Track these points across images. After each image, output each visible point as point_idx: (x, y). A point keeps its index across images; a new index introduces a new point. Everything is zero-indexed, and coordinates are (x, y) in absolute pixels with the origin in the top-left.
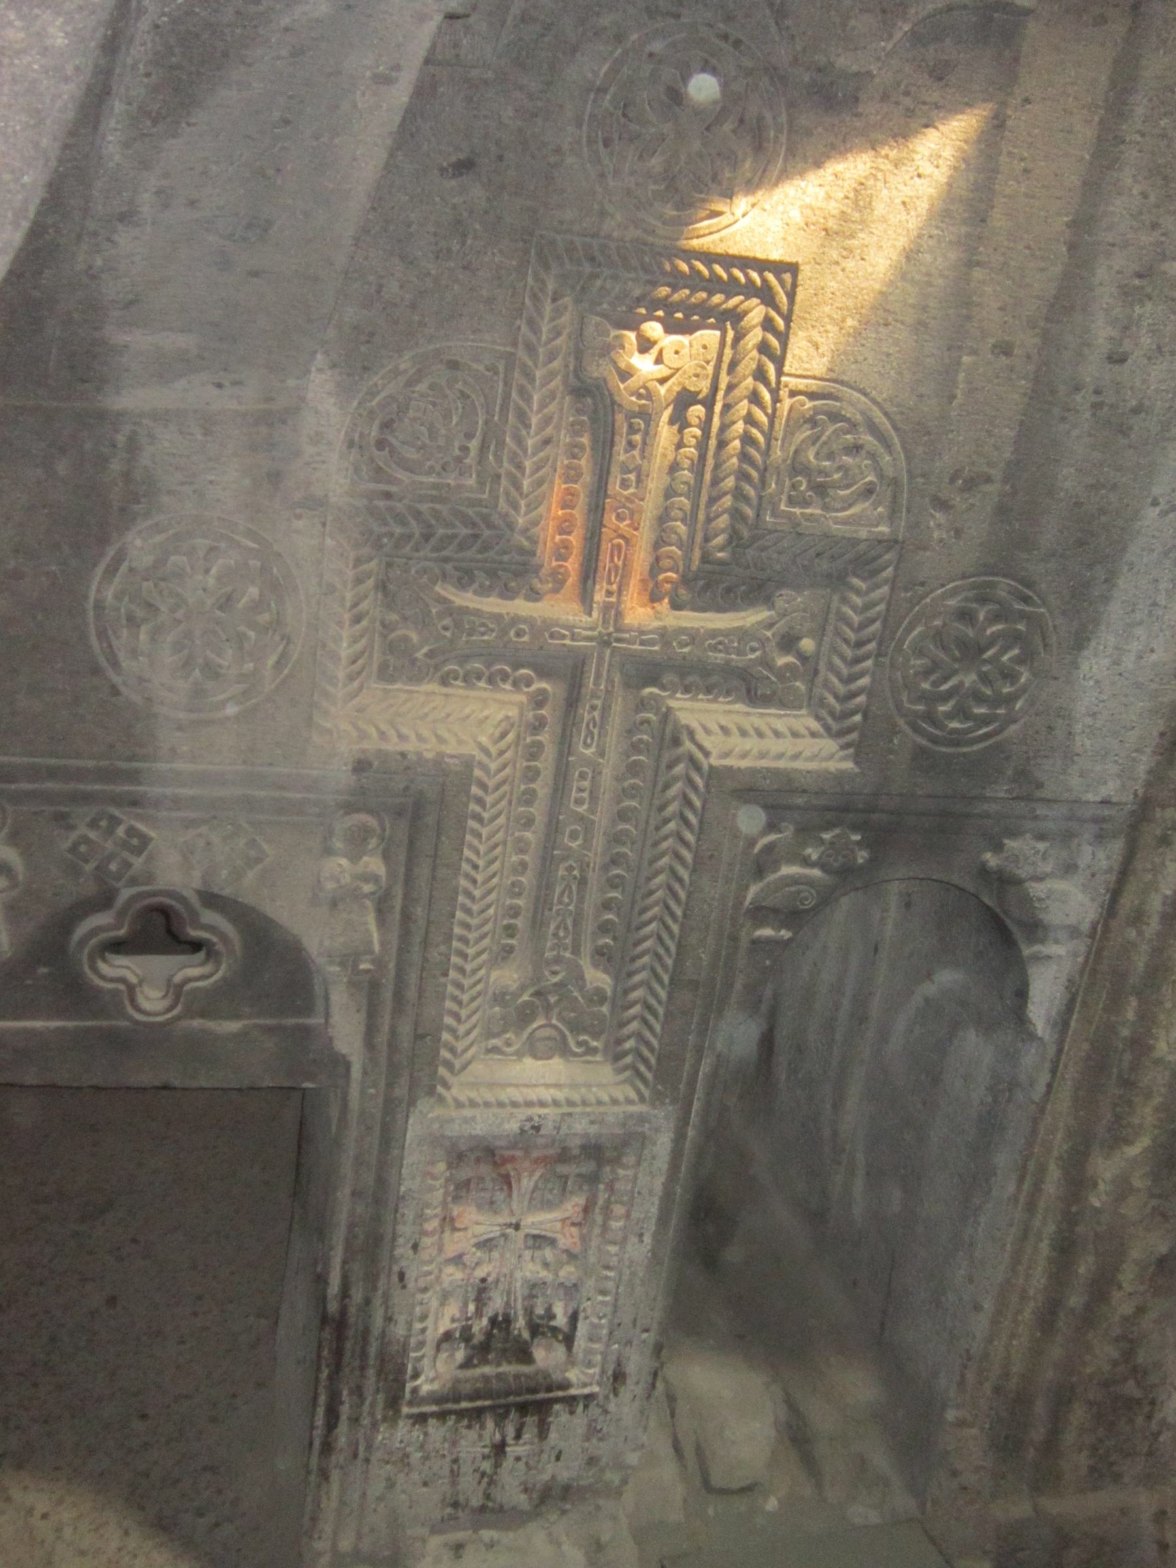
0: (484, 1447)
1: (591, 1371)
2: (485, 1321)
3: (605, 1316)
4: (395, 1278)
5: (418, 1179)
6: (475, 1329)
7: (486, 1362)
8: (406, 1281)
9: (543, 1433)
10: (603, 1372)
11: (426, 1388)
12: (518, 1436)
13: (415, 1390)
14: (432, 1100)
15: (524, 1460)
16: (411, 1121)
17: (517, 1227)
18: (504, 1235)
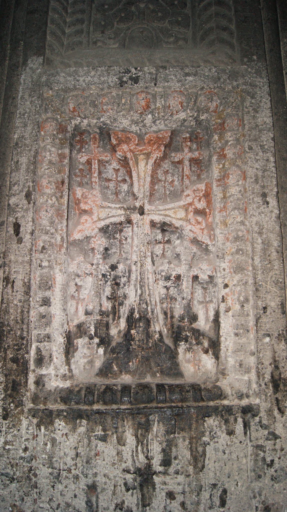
0: (127, 471)
1: (246, 378)
2: (123, 324)
3: (247, 300)
4: (11, 230)
5: (29, 128)
6: (113, 332)
7: (124, 369)
8: (21, 235)
9: (198, 460)
10: (259, 375)
11: (55, 383)
12: (166, 463)
13: (39, 382)
14: (41, 60)
15: (180, 498)
16: (23, 77)
17: (142, 212)
18: (129, 222)
